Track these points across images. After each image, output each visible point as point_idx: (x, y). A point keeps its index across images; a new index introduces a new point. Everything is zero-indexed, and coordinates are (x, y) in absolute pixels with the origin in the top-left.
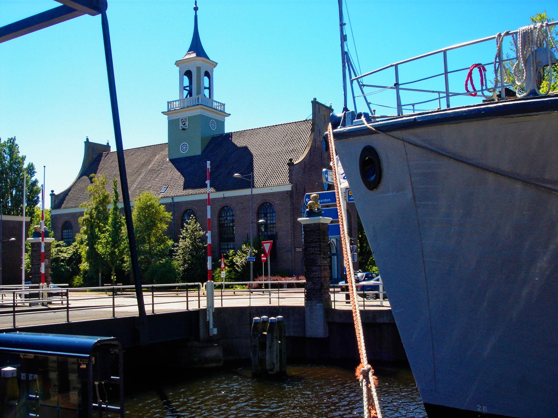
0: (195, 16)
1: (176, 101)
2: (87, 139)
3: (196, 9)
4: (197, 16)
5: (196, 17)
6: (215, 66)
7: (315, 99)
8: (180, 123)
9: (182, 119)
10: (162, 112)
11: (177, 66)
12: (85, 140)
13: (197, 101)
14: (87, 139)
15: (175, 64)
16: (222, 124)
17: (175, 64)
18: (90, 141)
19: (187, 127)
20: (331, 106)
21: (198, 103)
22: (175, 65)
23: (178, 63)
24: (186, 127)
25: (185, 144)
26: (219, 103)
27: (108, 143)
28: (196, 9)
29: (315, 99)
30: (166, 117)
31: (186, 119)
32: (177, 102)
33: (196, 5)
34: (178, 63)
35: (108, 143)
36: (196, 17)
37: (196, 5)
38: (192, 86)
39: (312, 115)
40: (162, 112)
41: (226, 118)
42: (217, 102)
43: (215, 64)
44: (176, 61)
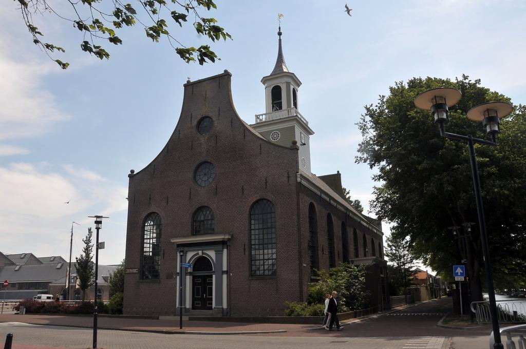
3: (280, 34)
5: (280, 40)
6: (299, 86)
23: (265, 80)
28: (280, 34)
32: (264, 116)
33: (280, 30)
34: (265, 80)
36: (280, 40)
37: (280, 30)
41: (310, 136)
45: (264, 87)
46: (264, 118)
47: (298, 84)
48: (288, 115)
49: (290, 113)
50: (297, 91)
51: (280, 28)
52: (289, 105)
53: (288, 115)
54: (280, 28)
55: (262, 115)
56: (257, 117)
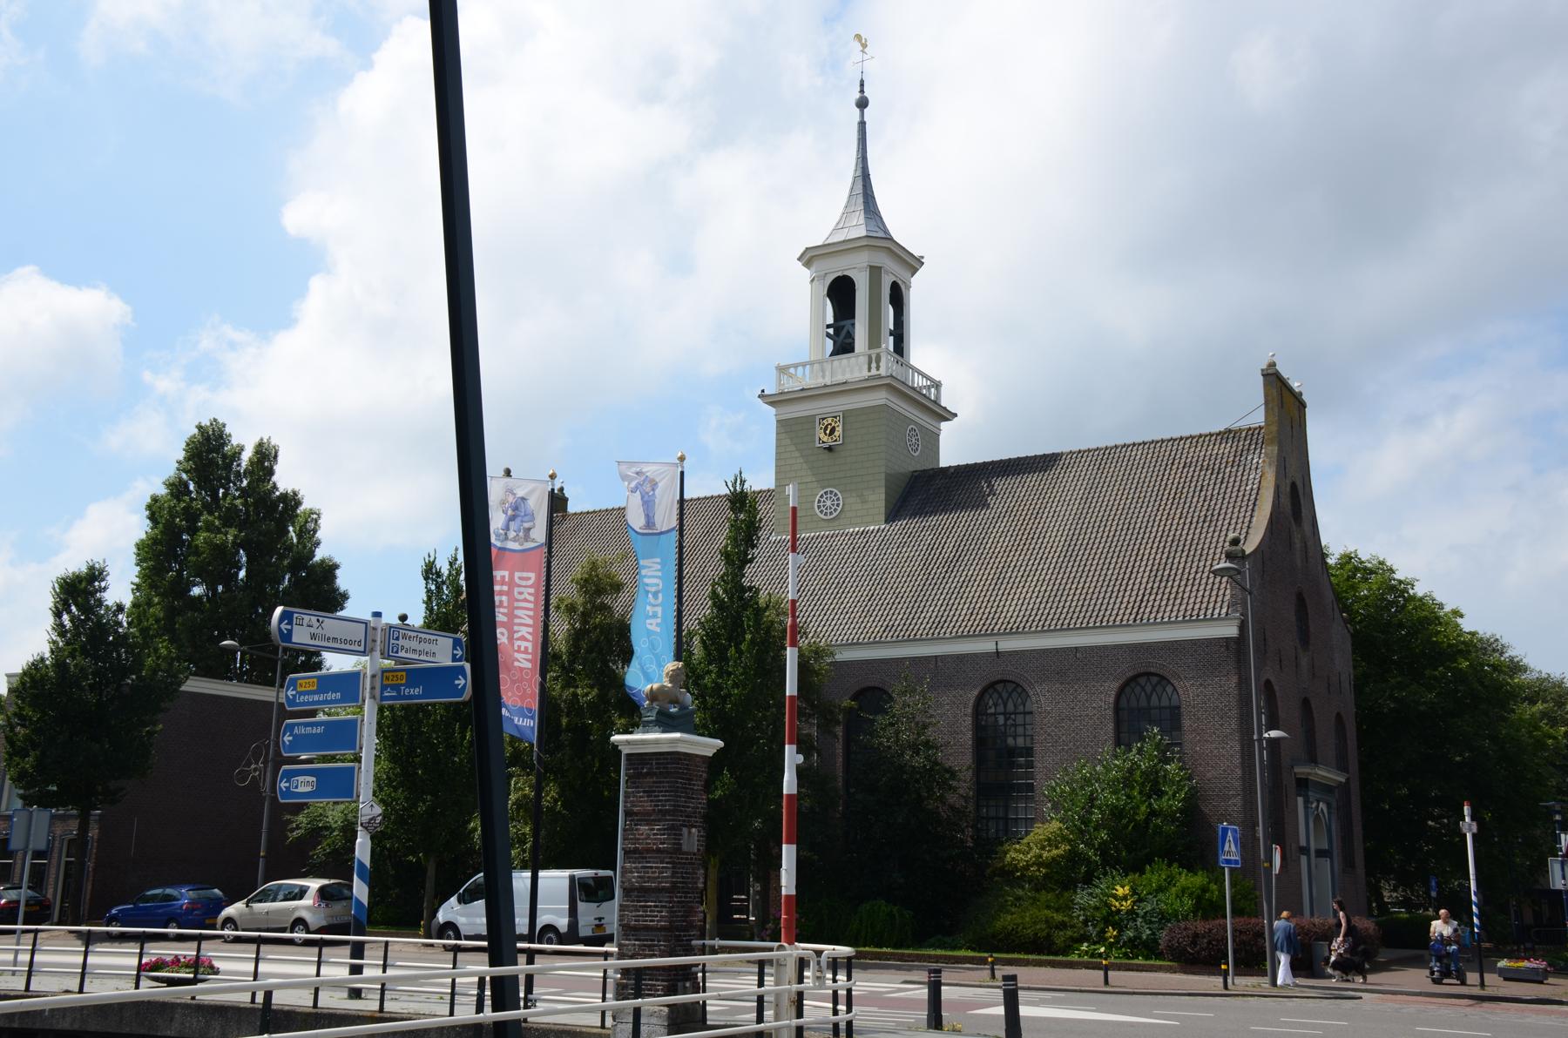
1: (804, 365)
3: (862, 104)
4: (865, 123)
5: (862, 124)
6: (914, 271)
7: (1272, 365)
8: (818, 428)
9: (823, 419)
11: (808, 264)
13: (874, 365)
15: (799, 259)
16: (934, 438)
17: (799, 259)
19: (841, 442)
21: (878, 373)
22: (800, 264)
23: (810, 257)
24: (836, 441)
25: (831, 492)
26: (928, 378)
28: (862, 104)
29: (1272, 365)
30: (772, 410)
31: (836, 417)
32: (800, 369)
33: (862, 91)
34: (810, 257)
36: (862, 124)
37: (862, 91)
38: (853, 325)
39: (1263, 407)
41: (944, 425)
43: (913, 264)
44: (807, 248)
45: (806, 274)
47: (913, 264)
48: (869, 370)
49: (874, 365)
50: (908, 287)
51: (862, 85)
52: (874, 341)
53: (869, 370)
54: (862, 85)
55: (796, 366)
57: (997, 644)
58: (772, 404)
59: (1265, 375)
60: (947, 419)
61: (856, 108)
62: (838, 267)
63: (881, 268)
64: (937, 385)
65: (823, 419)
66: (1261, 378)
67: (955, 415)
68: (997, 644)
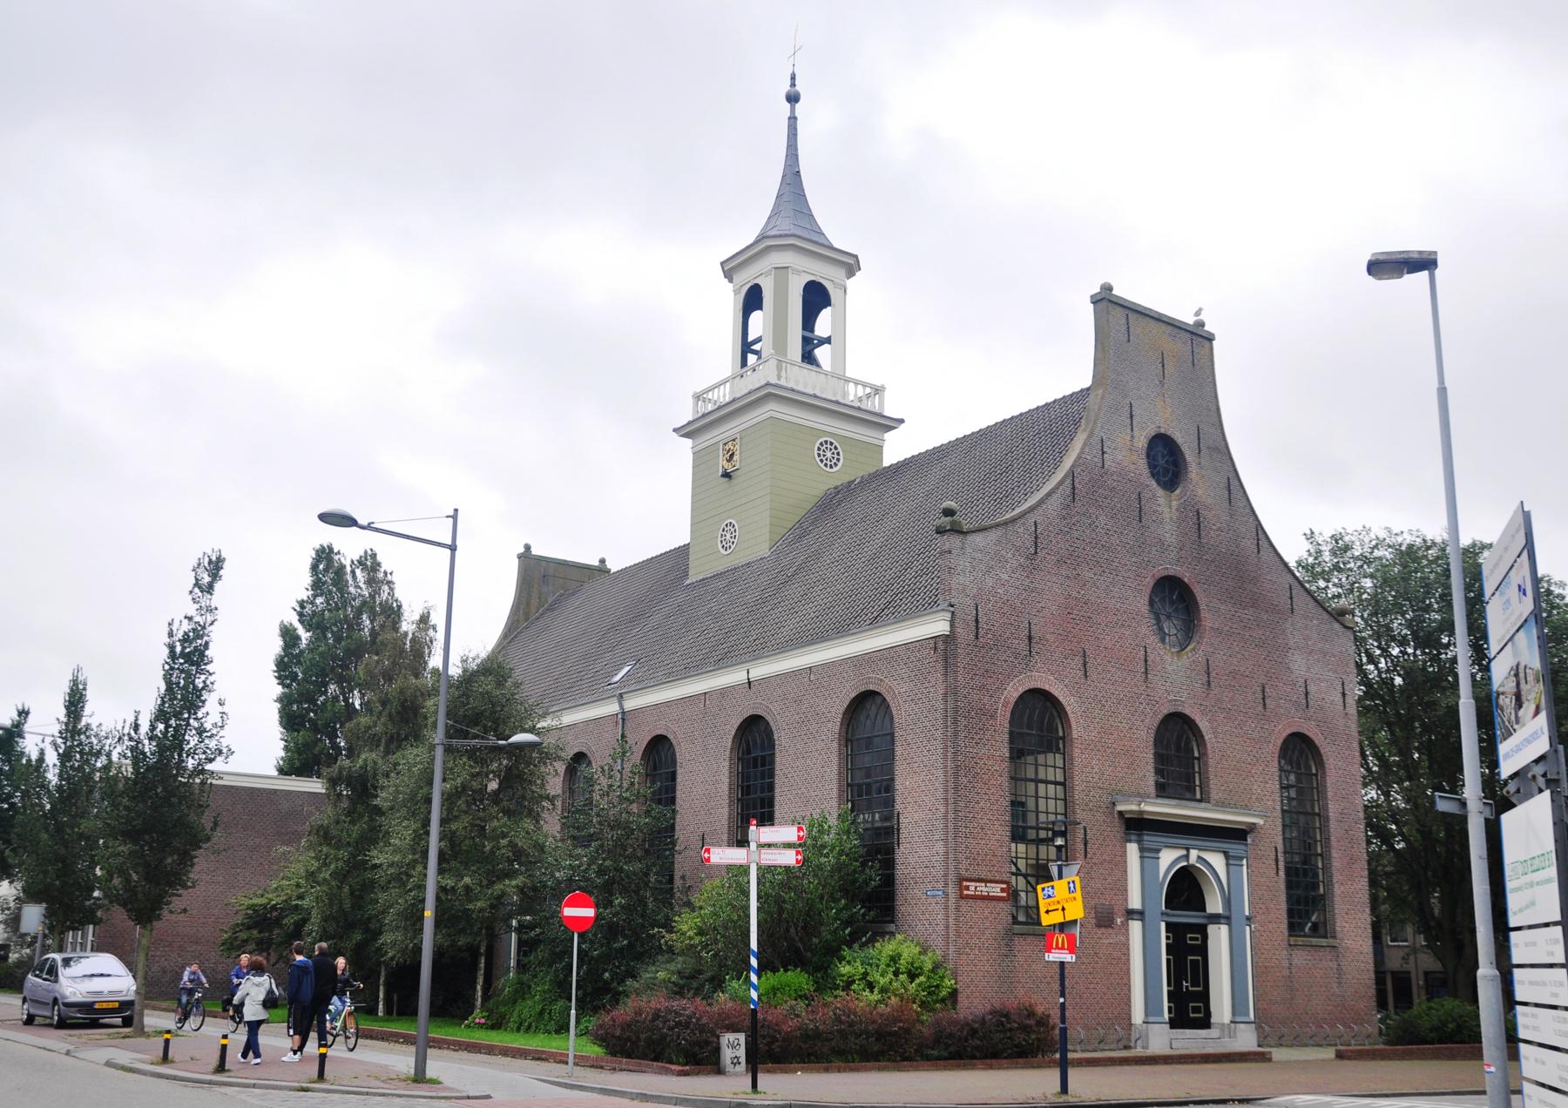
0: (789, 118)
2: (528, 547)
3: (793, 98)
5: (793, 119)
7: (1107, 288)
9: (725, 444)
10: (675, 430)
12: (522, 550)
14: (528, 547)
18: (535, 551)
20: (1201, 324)
23: (730, 269)
26: (865, 385)
27: (603, 561)
28: (793, 98)
29: (1107, 288)
30: (688, 442)
31: (734, 440)
33: (793, 85)
34: (730, 269)
35: (603, 561)
36: (793, 119)
37: (793, 85)
40: (675, 430)
41: (888, 436)
42: (857, 383)
46: (723, 395)
51: (793, 78)
54: (793, 78)
56: (698, 397)
57: (748, 672)
58: (687, 435)
59: (1096, 301)
60: (891, 428)
61: (786, 103)
62: (746, 278)
63: (788, 267)
64: (878, 391)
65: (725, 444)
66: (1090, 309)
67: (902, 421)
68: (748, 672)
